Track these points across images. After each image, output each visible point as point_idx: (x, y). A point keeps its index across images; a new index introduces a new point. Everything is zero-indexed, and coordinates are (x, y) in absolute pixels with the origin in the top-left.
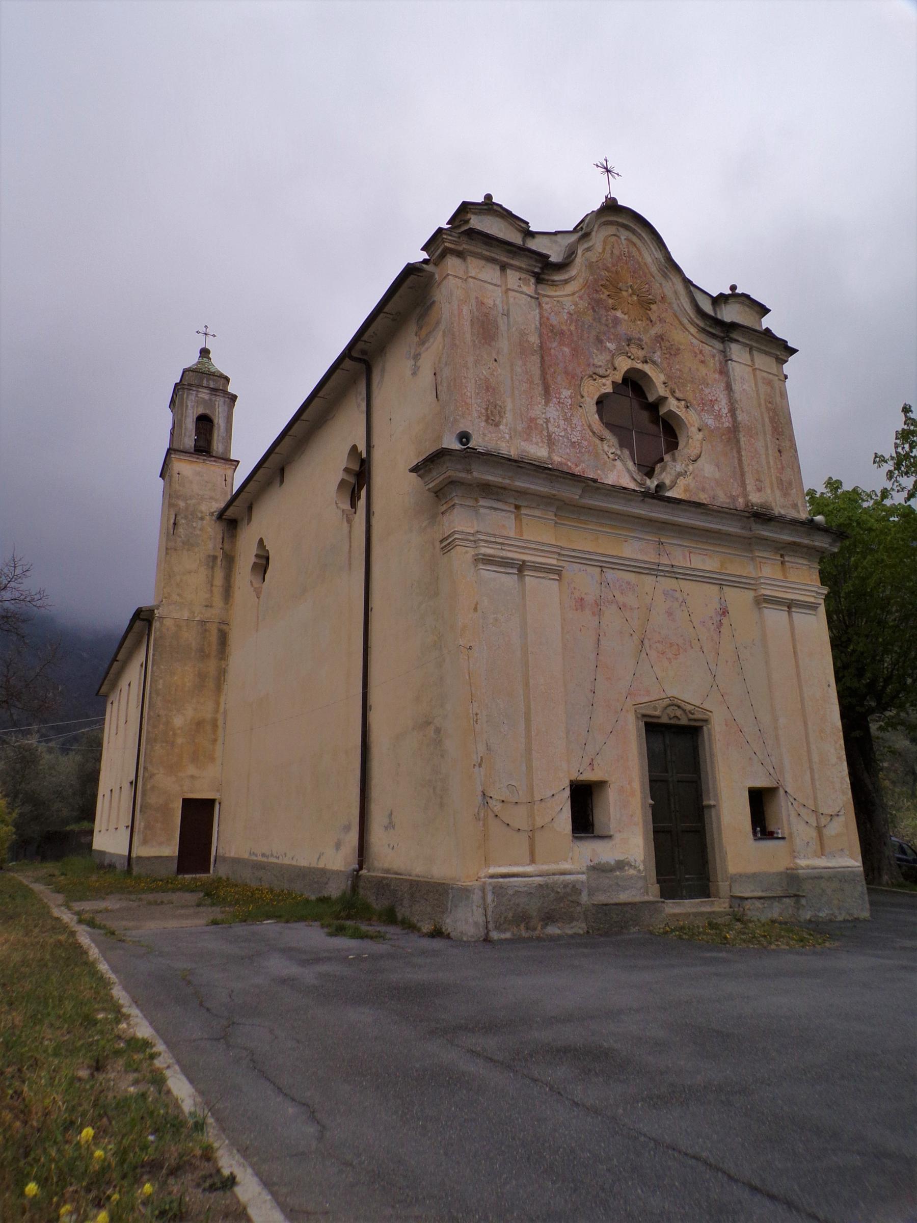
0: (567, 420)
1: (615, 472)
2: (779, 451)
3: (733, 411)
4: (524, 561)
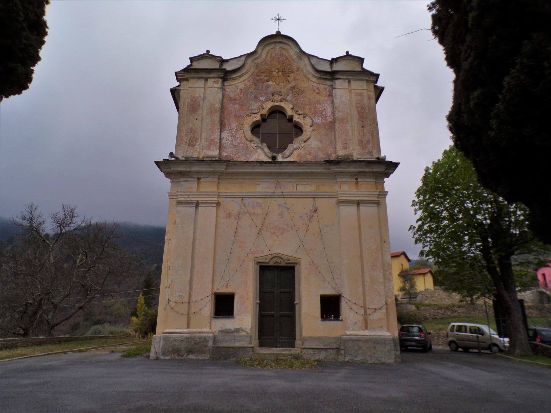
0: (233, 136)
1: (257, 154)
2: (363, 127)
3: (333, 113)
4: (198, 201)
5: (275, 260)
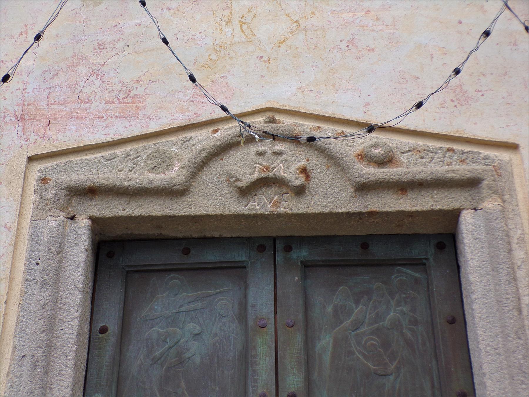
5: (244, 165)
